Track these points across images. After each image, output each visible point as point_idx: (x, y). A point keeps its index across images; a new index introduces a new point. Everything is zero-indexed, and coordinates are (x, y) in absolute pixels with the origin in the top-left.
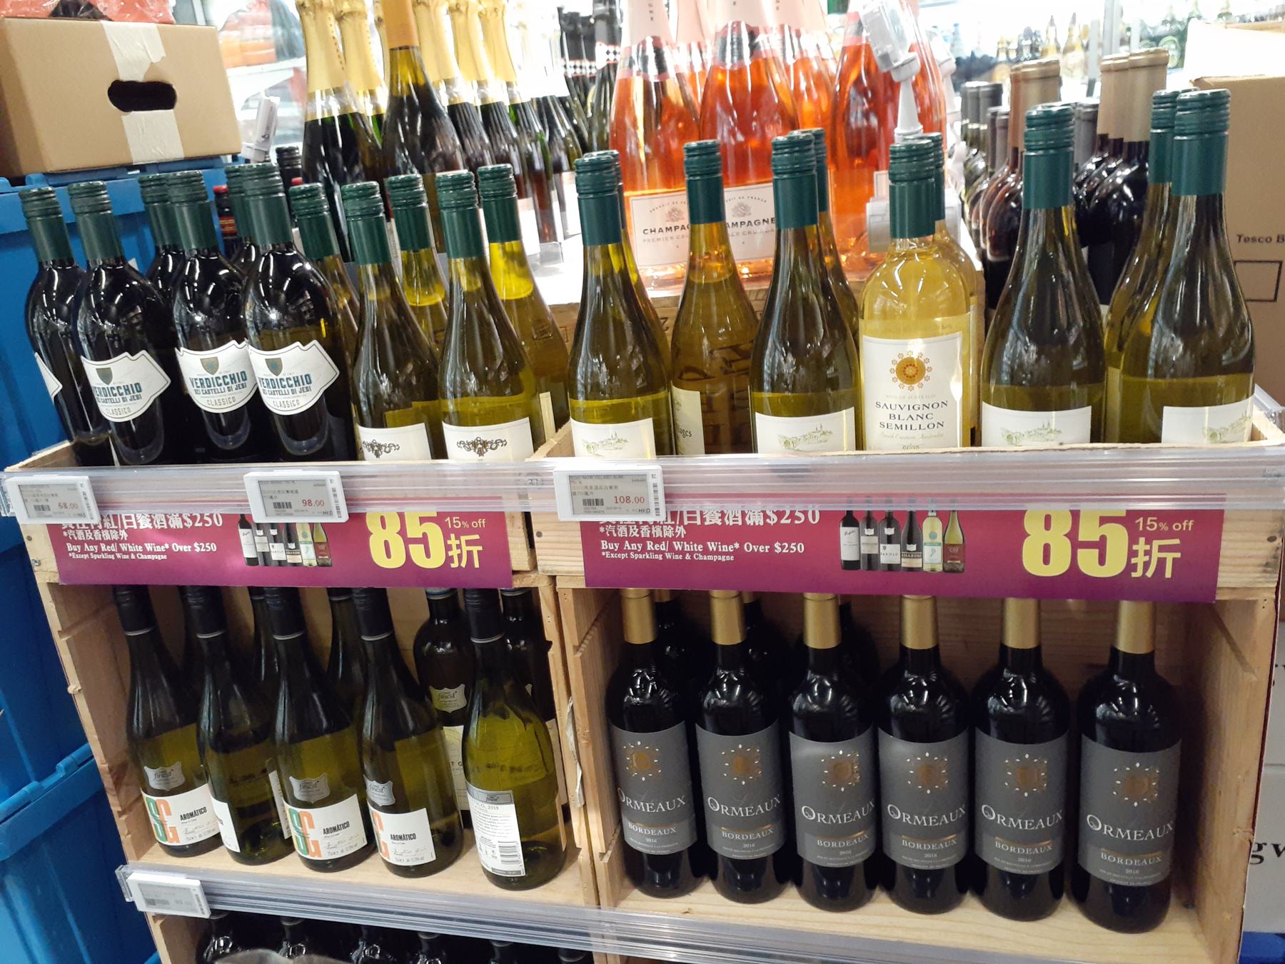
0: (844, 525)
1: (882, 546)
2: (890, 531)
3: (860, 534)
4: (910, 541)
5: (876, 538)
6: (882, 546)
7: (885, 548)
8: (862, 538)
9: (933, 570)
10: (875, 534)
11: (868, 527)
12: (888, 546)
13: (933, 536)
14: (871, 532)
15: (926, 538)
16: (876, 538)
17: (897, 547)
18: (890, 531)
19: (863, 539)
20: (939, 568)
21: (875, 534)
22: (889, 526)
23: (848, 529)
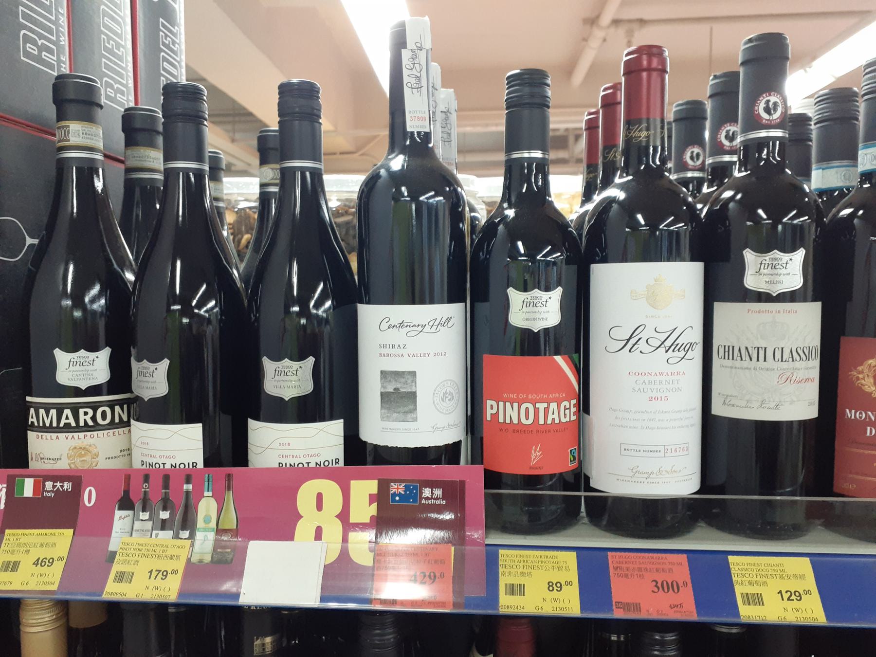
0: (120, 509)
1: (154, 532)
2: (165, 515)
3: (135, 518)
4: (184, 528)
5: (150, 523)
6: (154, 532)
7: (157, 535)
8: (136, 523)
9: (201, 561)
10: (150, 519)
11: (144, 510)
12: (161, 533)
13: (207, 520)
14: (145, 516)
15: (200, 523)
16: (150, 523)
17: (169, 533)
18: (165, 515)
19: (137, 525)
20: (208, 558)
21: (150, 519)
22: (165, 509)
23: (124, 513)
